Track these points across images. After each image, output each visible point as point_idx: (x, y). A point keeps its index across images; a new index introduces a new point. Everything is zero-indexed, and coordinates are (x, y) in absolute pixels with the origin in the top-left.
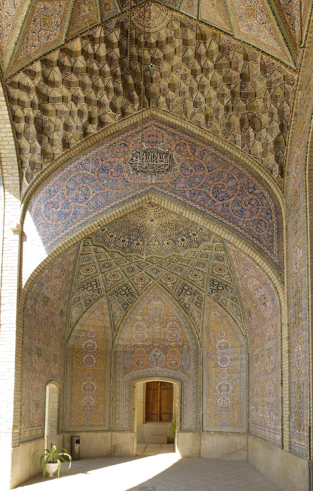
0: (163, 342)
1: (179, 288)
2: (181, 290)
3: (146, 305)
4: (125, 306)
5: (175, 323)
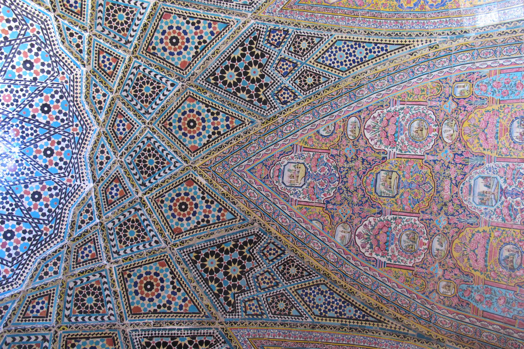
0: (437, 167)
1: (231, 99)
2: (243, 95)
3: (295, 207)
4: (293, 271)
5: (370, 122)
